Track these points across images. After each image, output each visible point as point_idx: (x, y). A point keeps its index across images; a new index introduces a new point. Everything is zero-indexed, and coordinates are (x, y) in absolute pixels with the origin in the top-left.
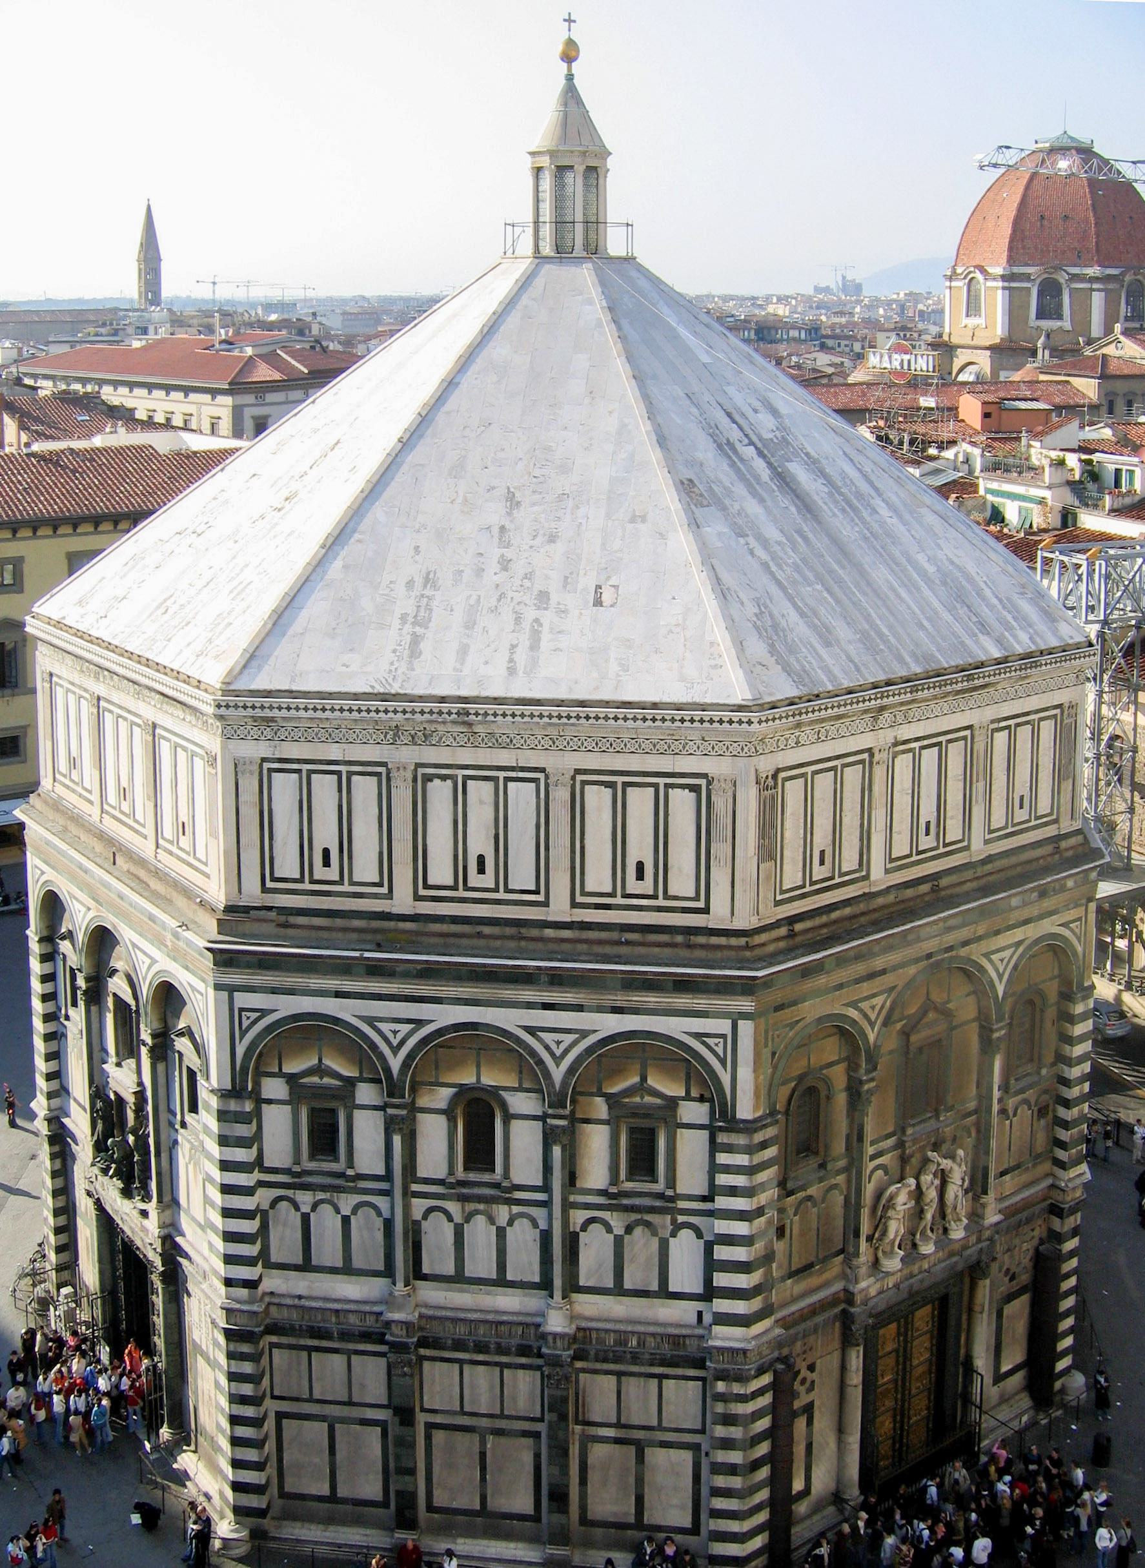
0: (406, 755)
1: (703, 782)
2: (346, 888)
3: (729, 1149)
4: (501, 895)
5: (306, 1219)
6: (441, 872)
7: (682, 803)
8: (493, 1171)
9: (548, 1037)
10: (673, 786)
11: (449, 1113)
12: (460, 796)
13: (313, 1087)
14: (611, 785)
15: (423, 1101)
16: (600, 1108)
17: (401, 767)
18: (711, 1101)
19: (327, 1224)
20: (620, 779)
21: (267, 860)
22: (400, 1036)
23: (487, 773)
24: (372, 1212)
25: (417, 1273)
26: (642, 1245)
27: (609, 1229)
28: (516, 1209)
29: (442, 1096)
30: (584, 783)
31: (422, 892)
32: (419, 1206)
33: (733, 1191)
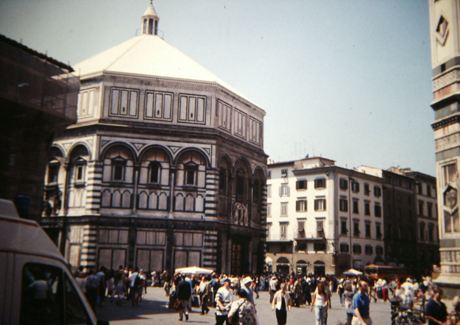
0: (144, 87)
1: (205, 97)
2: (128, 116)
3: (211, 174)
4: (162, 119)
5: (112, 195)
6: (150, 114)
7: (201, 101)
8: (156, 181)
9: (172, 148)
10: (199, 98)
11: (148, 168)
12: (154, 98)
13: (117, 161)
14: (187, 97)
15: (143, 165)
16: (182, 166)
17: (142, 90)
18: (206, 166)
19: (117, 196)
20: (188, 96)
21: (110, 109)
22: (140, 147)
23: (161, 93)
24: (128, 193)
25: (138, 208)
26: (190, 199)
27: (182, 196)
28: (162, 191)
29: (147, 164)
30: (181, 96)
31: (145, 118)
32: (140, 190)
33: (211, 184)
